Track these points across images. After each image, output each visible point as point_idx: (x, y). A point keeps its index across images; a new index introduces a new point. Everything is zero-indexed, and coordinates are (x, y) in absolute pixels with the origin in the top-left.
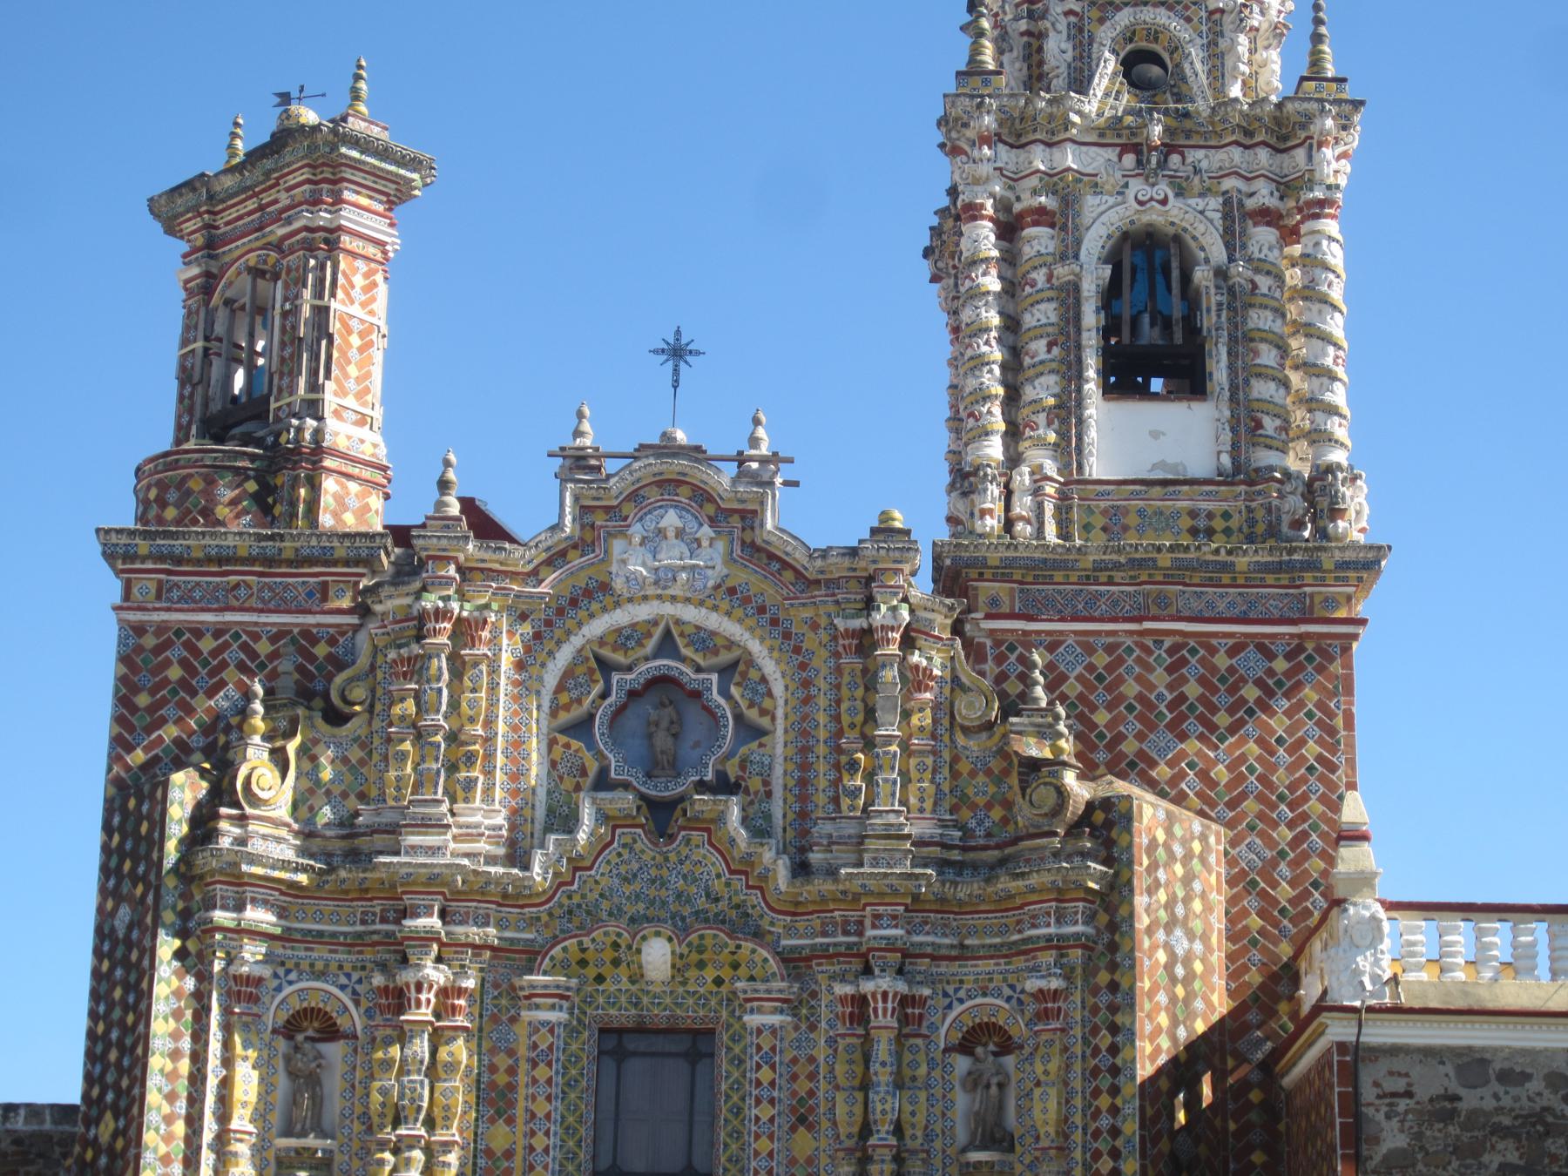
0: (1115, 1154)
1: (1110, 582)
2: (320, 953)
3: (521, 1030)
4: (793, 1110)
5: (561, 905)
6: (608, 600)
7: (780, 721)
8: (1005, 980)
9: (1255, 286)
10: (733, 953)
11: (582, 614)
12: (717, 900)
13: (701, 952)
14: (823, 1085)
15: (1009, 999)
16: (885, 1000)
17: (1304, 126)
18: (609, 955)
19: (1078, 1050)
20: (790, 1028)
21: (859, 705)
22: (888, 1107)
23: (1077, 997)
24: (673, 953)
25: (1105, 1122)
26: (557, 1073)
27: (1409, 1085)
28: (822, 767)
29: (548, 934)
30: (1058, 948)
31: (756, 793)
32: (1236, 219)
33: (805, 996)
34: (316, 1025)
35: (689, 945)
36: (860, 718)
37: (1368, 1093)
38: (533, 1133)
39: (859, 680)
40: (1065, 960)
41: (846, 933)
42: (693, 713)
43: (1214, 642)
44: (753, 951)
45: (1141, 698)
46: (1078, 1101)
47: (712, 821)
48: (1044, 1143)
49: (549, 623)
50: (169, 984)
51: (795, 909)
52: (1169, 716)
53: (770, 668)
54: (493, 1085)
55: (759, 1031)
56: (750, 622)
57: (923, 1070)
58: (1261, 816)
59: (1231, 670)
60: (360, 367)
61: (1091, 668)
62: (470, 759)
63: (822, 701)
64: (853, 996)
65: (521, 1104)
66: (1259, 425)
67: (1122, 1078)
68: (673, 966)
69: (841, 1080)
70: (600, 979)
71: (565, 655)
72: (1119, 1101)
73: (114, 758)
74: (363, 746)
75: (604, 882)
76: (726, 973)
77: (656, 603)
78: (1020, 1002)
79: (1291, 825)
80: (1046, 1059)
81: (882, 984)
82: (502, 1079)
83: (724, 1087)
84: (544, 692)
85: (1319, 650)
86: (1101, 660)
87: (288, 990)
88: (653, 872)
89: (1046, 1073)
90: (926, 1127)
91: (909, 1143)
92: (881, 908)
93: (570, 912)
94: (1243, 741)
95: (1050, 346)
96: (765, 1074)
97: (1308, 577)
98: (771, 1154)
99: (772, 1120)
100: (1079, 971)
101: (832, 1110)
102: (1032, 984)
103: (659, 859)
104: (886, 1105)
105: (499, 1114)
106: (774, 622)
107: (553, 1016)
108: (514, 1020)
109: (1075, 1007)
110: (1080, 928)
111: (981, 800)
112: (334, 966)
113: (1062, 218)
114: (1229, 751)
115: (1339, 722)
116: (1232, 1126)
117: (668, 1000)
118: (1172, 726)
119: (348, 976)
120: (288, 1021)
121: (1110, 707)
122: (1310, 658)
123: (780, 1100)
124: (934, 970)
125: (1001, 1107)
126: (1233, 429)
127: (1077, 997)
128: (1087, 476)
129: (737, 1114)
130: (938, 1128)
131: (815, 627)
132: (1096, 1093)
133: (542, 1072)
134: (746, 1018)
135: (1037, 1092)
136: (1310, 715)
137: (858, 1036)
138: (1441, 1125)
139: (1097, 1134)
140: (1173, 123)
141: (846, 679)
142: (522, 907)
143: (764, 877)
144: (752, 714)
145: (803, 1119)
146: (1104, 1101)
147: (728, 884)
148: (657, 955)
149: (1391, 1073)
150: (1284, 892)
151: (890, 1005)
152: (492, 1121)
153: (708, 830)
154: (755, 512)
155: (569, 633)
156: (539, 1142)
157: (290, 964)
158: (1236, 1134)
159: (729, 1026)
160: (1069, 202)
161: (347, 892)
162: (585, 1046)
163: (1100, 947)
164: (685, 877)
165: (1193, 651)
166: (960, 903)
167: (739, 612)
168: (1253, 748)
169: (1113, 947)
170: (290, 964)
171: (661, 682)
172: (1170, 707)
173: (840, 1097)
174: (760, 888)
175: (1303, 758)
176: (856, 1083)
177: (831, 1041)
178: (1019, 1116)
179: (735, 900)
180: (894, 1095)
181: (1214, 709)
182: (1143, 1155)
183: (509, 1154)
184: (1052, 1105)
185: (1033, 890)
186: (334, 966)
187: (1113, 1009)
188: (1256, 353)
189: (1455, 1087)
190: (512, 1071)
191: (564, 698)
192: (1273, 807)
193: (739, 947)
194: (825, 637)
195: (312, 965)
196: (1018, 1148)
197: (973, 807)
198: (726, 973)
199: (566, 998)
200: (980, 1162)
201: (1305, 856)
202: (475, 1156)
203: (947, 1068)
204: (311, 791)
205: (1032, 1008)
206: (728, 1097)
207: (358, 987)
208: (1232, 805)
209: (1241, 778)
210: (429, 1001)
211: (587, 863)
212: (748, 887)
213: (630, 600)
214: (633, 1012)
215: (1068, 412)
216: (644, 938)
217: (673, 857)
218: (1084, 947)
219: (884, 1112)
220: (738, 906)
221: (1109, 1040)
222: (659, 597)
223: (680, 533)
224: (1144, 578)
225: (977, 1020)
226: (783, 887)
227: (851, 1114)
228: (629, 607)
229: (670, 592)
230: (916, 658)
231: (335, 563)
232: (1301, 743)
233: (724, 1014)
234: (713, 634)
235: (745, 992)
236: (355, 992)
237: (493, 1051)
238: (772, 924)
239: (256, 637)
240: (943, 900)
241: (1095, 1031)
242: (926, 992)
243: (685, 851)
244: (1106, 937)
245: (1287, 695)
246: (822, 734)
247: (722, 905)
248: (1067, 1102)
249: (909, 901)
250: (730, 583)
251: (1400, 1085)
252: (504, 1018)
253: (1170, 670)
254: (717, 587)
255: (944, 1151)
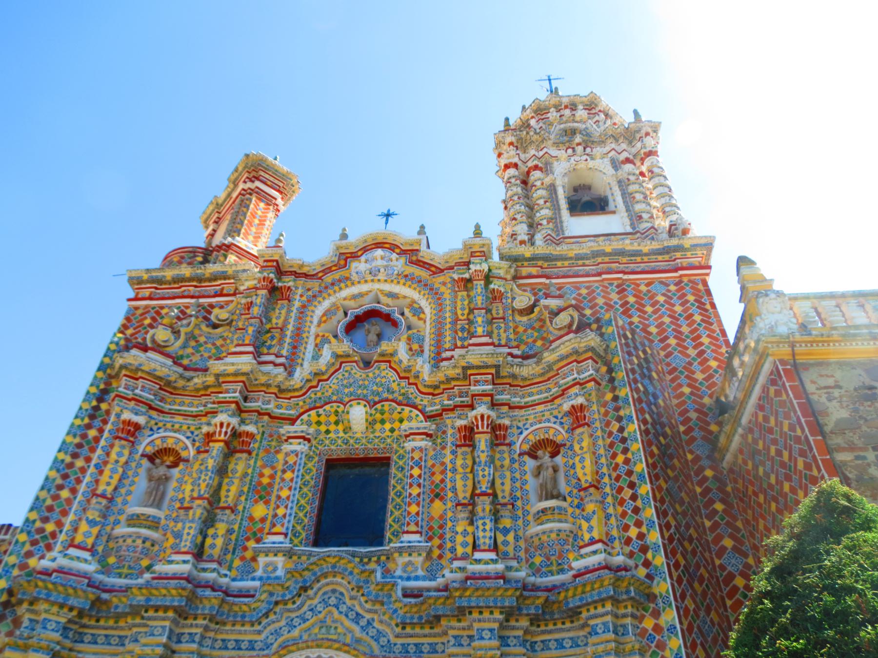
0: (632, 485)
1: (584, 265)
2: (179, 419)
3: (280, 457)
4: (432, 491)
5: (310, 398)
6: (349, 283)
7: (428, 323)
8: (551, 414)
9: (628, 180)
10: (400, 413)
11: (336, 288)
12: (393, 392)
13: (382, 414)
14: (449, 475)
15: (555, 423)
16: (482, 419)
17: (639, 131)
18: (333, 418)
19: (599, 433)
20: (431, 449)
21: (467, 308)
22: (486, 473)
23: (595, 408)
24: (366, 413)
25: (623, 469)
26: (298, 476)
27: (836, 381)
28: (448, 333)
29: (302, 410)
30: (581, 384)
31: (416, 351)
32: (616, 165)
33: (439, 434)
34: (171, 459)
35: (376, 409)
36: (466, 312)
37: (810, 388)
38: (278, 507)
39: (466, 297)
40: (585, 390)
41: (460, 397)
42: (389, 330)
43: (638, 282)
44: (411, 411)
45: (605, 304)
46: (603, 460)
47: (392, 355)
48: (585, 485)
49: (320, 292)
50: (82, 419)
51: (434, 390)
52: (622, 310)
53: (424, 303)
54: (260, 483)
55: (413, 450)
56: (415, 285)
57: (507, 462)
58: (677, 344)
59: (649, 291)
60: (257, 229)
61: (580, 295)
62: (272, 338)
63: (448, 308)
64: (465, 426)
65: (275, 493)
66: (640, 217)
67: (629, 441)
68: (367, 420)
69: (460, 470)
70: (328, 432)
71: (326, 304)
72: (629, 455)
73: (108, 353)
74: (225, 340)
75: (334, 387)
76: (396, 425)
77: (371, 284)
78: (561, 423)
79: (695, 347)
80: (580, 441)
81: (482, 409)
82: (265, 480)
83: (393, 482)
84: (315, 317)
85: (690, 281)
86: (584, 291)
87: (156, 436)
88: (361, 383)
89: (581, 448)
90: (511, 494)
91: (502, 501)
92: (479, 377)
93: (315, 401)
94: (661, 317)
95: (545, 202)
96: (416, 472)
97: (678, 255)
98: (418, 514)
99: (419, 495)
100: (594, 394)
101: (454, 489)
102: (566, 407)
103: (364, 376)
104: (485, 475)
105: (261, 498)
106: (426, 285)
107: (298, 448)
108: (278, 452)
109: (595, 413)
110: (591, 372)
111: (530, 340)
112: (185, 427)
113: (545, 168)
114: (656, 319)
115: (708, 307)
116: (698, 490)
117: (364, 441)
118: (624, 313)
119: (192, 433)
120: (154, 454)
121: (591, 308)
122: (686, 284)
123: (424, 486)
124: (511, 414)
125: (555, 480)
126: (630, 220)
127: (595, 408)
128: (567, 235)
129: (400, 495)
130: (518, 494)
131: (444, 284)
132: (614, 456)
133: (288, 475)
134: (406, 444)
135: (577, 459)
136: (693, 305)
137: (469, 446)
138: (869, 403)
139: (618, 478)
140: (585, 138)
141: (459, 297)
142: (289, 399)
143: (417, 377)
144: (414, 320)
145: (438, 496)
146: (620, 459)
147: (399, 385)
148: (358, 414)
149: (821, 376)
150: (699, 376)
151: (485, 422)
152: (256, 502)
153: (389, 362)
154: (417, 250)
155: (329, 295)
156: (281, 512)
157: (160, 424)
158: (701, 494)
159: (397, 452)
160: (547, 164)
161: (197, 390)
162: (315, 467)
163: (604, 383)
164: (377, 384)
165: (629, 286)
166: (525, 379)
167: (409, 283)
168: (667, 320)
169: (612, 380)
170: (160, 424)
171: (372, 314)
172: (622, 306)
173: (458, 477)
174: (416, 384)
175: (694, 322)
176: (469, 470)
177: (453, 453)
178: (568, 482)
179: (403, 391)
180: (490, 467)
181: (644, 306)
182: (651, 482)
183: (263, 520)
184: (587, 463)
185: (562, 358)
186: (185, 427)
187: (617, 409)
188: (634, 198)
189: (868, 382)
190: (272, 477)
191: (325, 318)
192: (684, 341)
193: (403, 410)
194: (449, 285)
195: (173, 426)
196: (569, 499)
197: (526, 343)
198: (396, 425)
199: (309, 440)
200: (546, 509)
201: (706, 360)
202: (242, 519)
203: (522, 464)
204: (193, 354)
205: (568, 421)
206: (394, 487)
207: (196, 438)
208: (661, 341)
209: (665, 330)
210: (226, 433)
211: (325, 377)
212: (410, 384)
213: (359, 282)
214: (344, 447)
215: (555, 220)
216: (351, 406)
217: (371, 375)
218: (594, 380)
219: (484, 476)
220: (404, 394)
221: (617, 425)
222: (372, 281)
223: (382, 258)
224: (600, 260)
225: (538, 438)
226: (426, 378)
227: (465, 486)
228: (359, 286)
229: (379, 277)
230: (492, 286)
231: (229, 279)
232: (692, 315)
233: (395, 446)
234: (397, 294)
235: (405, 431)
236: (194, 441)
237: (264, 466)
238: (422, 400)
239: (187, 307)
240: (514, 376)
241: (608, 424)
242: (506, 422)
243: (377, 372)
244: (607, 377)
245: (680, 298)
246: (449, 320)
247: (396, 395)
248: (596, 462)
249: (493, 371)
250: (405, 273)
251: (830, 382)
252: (272, 451)
253: (618, 293)
254: (398, 275)
255: (523, 508)
